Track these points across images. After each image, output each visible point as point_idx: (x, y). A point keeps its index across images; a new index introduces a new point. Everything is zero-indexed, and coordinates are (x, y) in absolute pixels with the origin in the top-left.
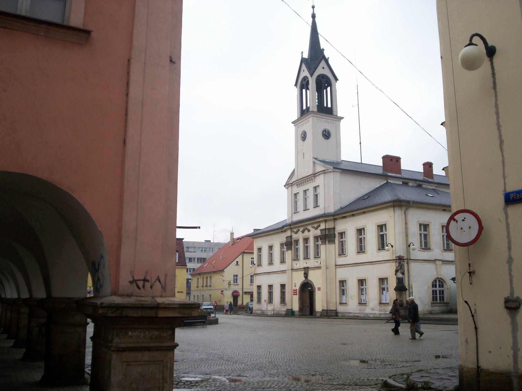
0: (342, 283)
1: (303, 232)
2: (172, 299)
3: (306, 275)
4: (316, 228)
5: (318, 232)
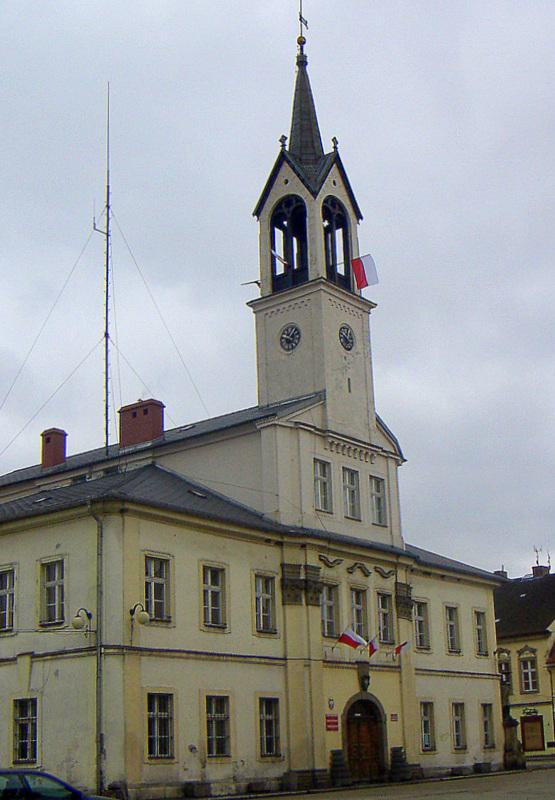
0: (427, 706)
1: (350, 571)
2: (340, 720)
3: (364, 681)
4: (384, 576)
5: (388, 586)
